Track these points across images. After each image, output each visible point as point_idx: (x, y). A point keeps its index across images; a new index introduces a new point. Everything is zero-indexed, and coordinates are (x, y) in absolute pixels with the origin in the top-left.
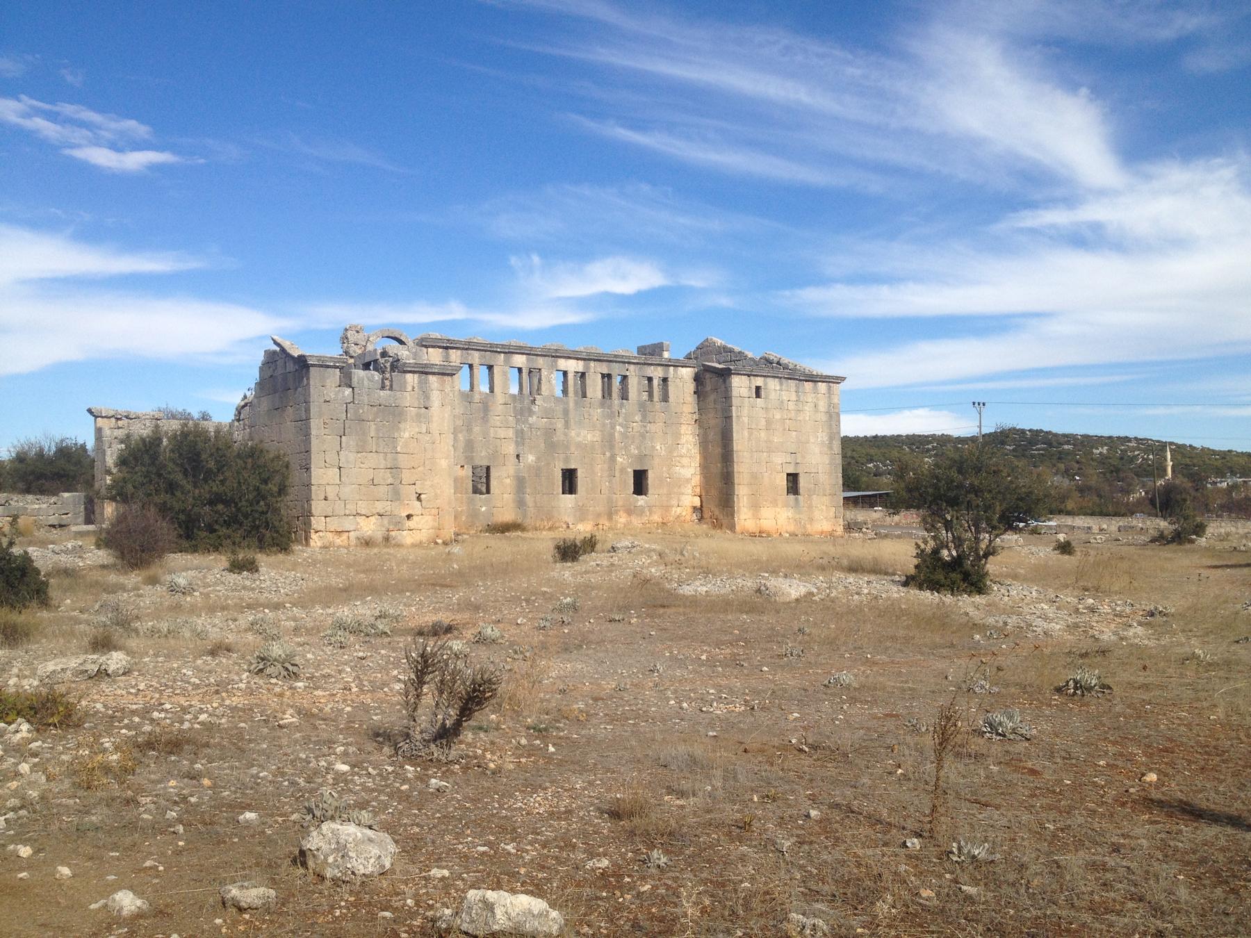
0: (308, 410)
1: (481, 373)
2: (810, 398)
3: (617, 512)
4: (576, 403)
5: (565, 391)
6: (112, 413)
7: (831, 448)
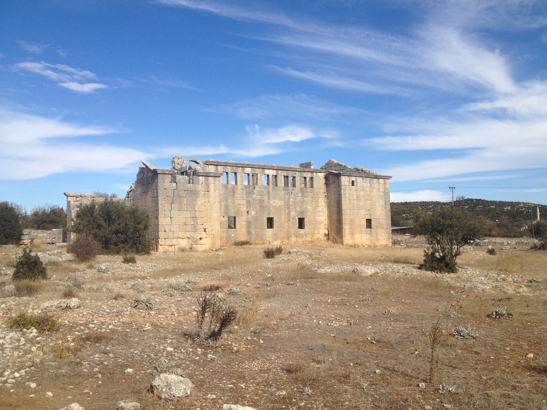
0: (157, 193)
1: (231, 176)
2: (376, 185)
3: (291, 236)
4: (273, 189)
5: (268, 184)
7: (386, 208)
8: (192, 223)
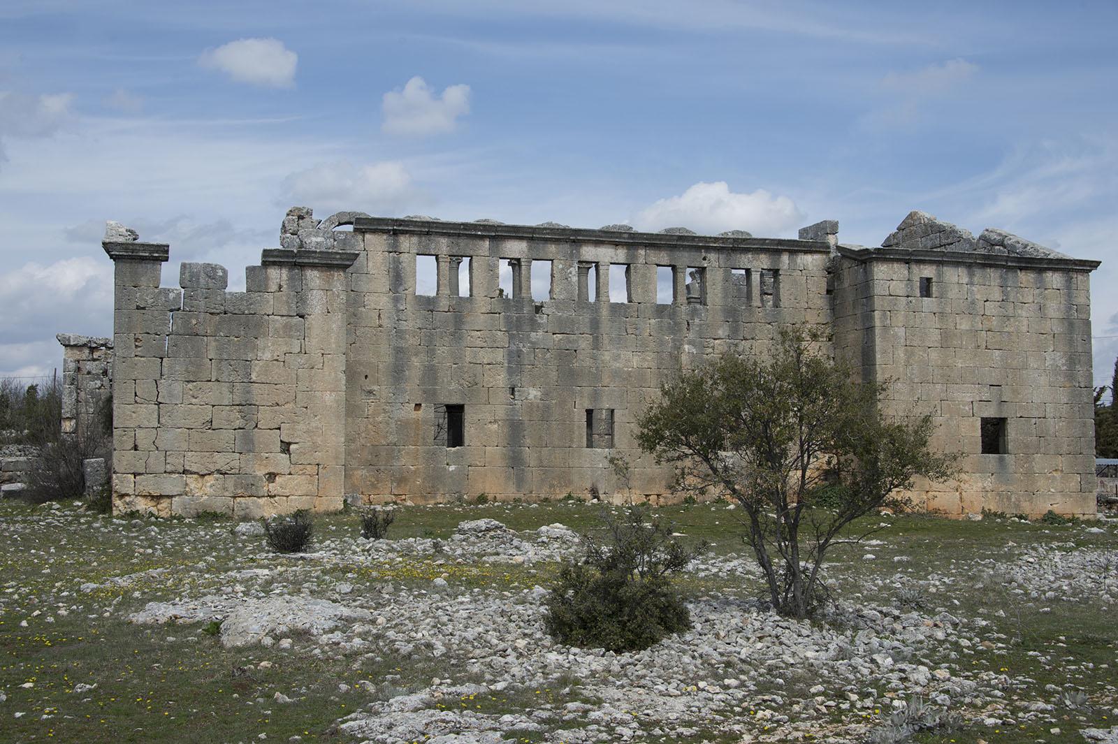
6: (84, 340)
8: (238, 423)
